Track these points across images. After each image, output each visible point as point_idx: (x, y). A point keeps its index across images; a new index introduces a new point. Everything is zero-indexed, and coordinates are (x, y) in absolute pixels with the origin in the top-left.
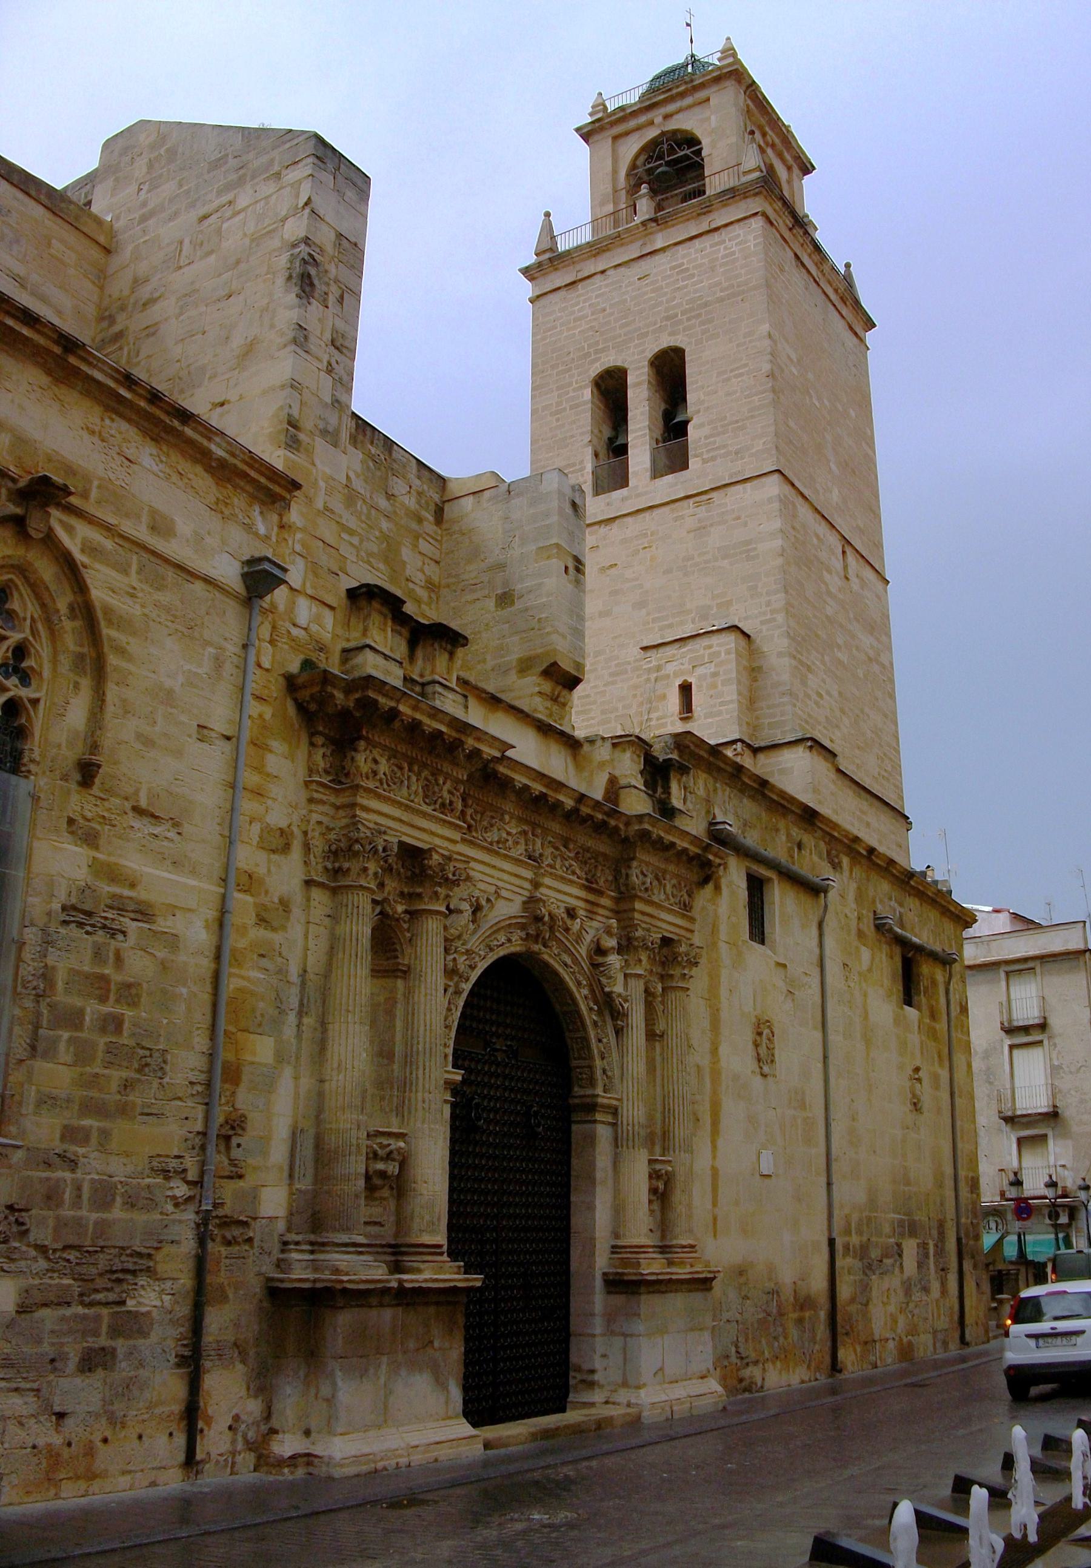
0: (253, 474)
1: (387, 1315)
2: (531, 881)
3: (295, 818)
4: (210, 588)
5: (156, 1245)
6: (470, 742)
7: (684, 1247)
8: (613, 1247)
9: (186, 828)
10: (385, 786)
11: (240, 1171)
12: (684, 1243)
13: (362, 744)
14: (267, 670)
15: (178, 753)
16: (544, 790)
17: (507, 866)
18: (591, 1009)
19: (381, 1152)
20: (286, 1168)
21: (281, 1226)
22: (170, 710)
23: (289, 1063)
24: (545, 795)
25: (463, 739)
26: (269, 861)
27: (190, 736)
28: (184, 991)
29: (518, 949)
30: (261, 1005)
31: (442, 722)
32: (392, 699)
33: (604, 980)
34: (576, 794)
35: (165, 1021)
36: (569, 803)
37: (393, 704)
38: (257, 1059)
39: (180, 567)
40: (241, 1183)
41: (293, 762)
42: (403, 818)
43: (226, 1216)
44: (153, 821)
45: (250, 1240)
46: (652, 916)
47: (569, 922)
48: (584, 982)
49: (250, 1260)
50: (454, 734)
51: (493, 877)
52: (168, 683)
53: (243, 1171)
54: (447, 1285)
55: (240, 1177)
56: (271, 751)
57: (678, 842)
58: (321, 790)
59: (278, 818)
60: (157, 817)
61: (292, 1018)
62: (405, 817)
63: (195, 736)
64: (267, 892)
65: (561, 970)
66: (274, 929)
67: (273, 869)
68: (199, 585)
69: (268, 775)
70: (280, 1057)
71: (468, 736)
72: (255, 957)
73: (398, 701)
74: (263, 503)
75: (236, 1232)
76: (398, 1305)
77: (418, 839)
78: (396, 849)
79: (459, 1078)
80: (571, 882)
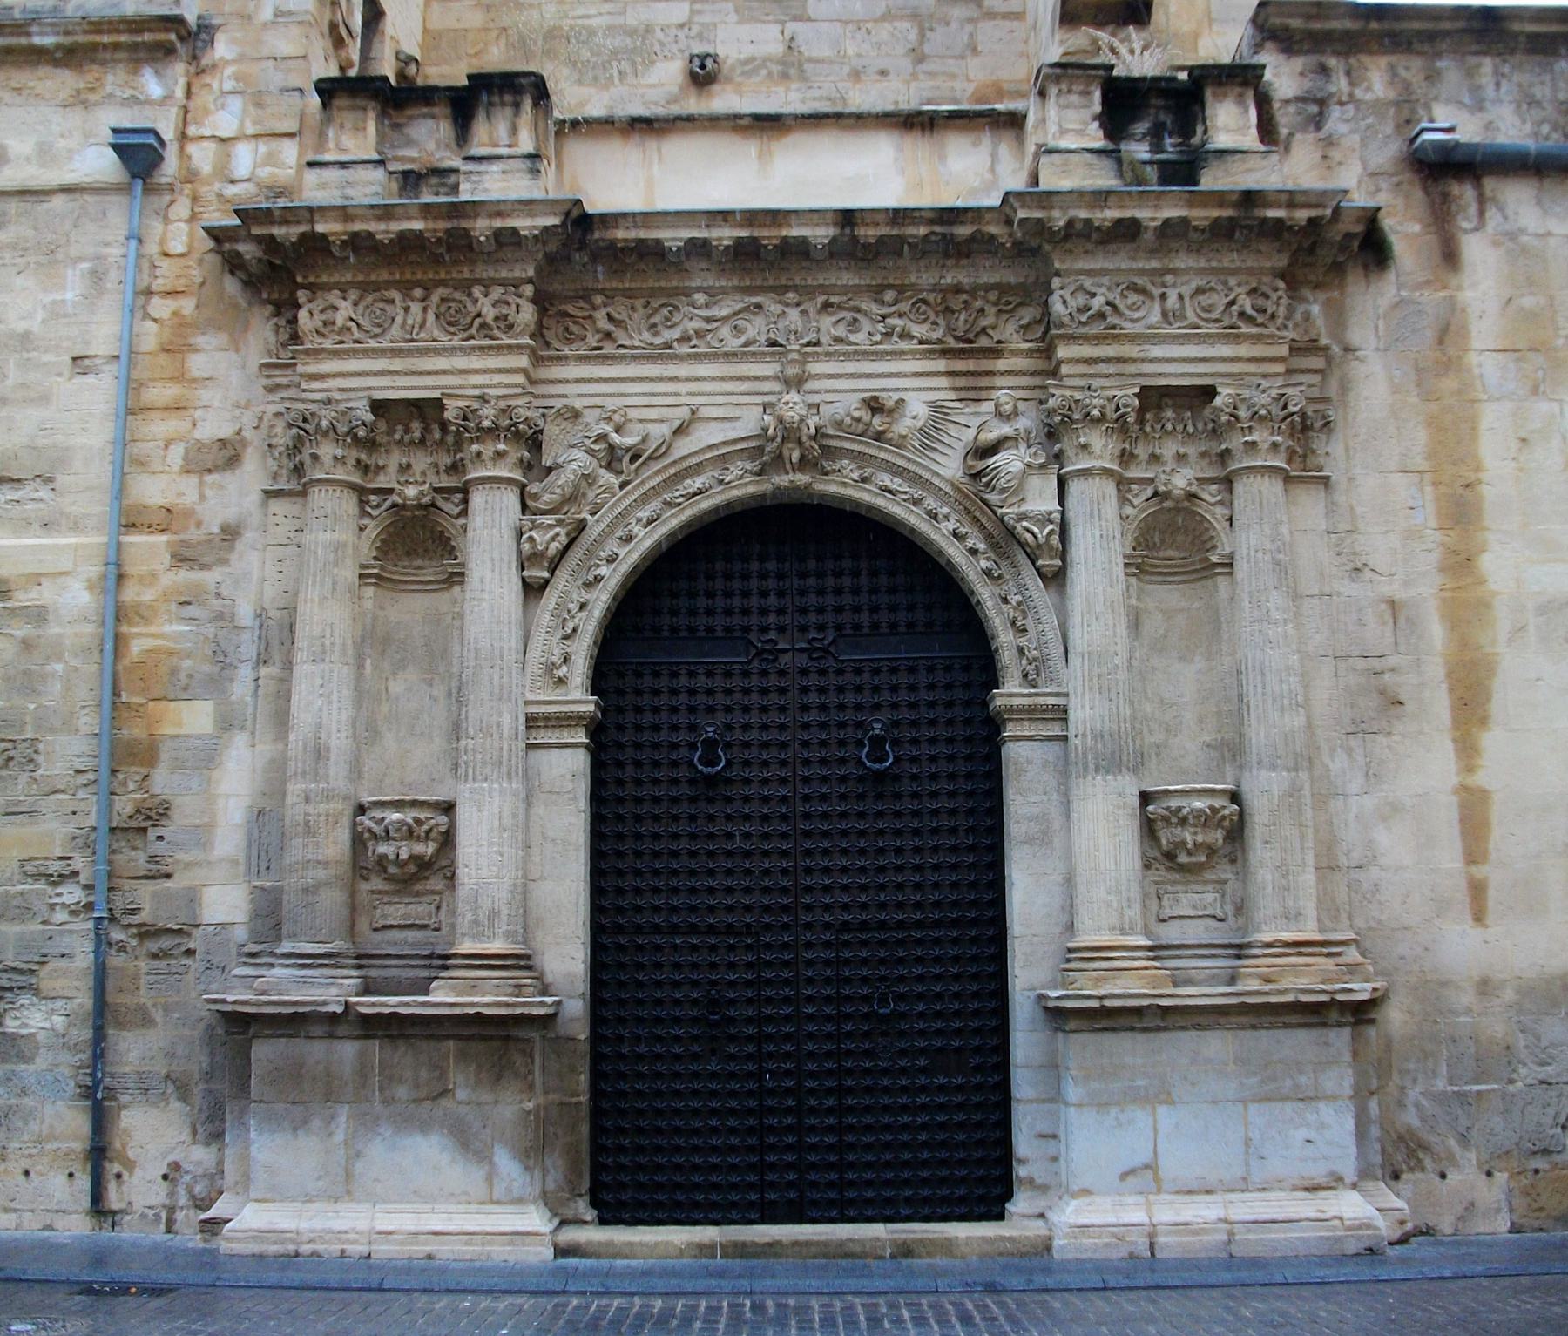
0: (106, 39)
1: (347, 1051)
2: (776, 378)
3: (248, 419)
4: (77, 196)
5: (37, 959)
6: (481, 227)
7: (1269, 945)
8: (1070, 950)
9: (62, 480)
10: (357, 335)
11: (164, 869)
12: (1267, 938)
13: (302, 296)
14: (182, 255)
15: (44, 399)
16: (744, 233)
17: (703, 370)
18: (973, 552)
19: (376, 828)
20: (242, 860)
21: (241, 934)
22: (26, 355)
23: (243, 728)
24: (754, 240)
25: (465, 224)
26: (201, 483)
27: (60, 375)
28: (59, 667)
29: (751, 489)
30: (187, 663)
31: (409, 218)
32: (298, 223)
33: (993, 498)
34: (830, 216)
35: (32, 706)
36: (821, 234)
37: (303, 228)
38: (183, 732)
39: (23, 193)
40: (168, 884)
41: (237, 350)
42: (392, 368)
43: (144, 924)
44: (16, 485)
45: (190, 953)
46: (1134, 360)
47: (877, 422)
48: (945, 510)
49: (191, 977)
50: (442, 225)
51: (677, 394)
52: (21, 326)
53: (169, 869)
54: (458, 1011)
55: (168, 876)
56: (197, 351)
57: (1142, 214)
58: (277, 372)
59: (213, 426)
60: (19, 480)
61: (245, 672)
62: (397, 364)
63: (67, 373)
64: (199, 525)
65: (880, 502)
66: (206, 567)
67: (209, 493)
68: (58, 202)
69: (194, 380)
70: (227, 724)
71: (476, 216)
72: (173, 607)
73: (312, 222)
74: (151, 60)
75: (165, 943)
76: (367, 1037)
77: (428, 388)
78: (369, 417)
79: (592, 708)
80: (898, 354)
